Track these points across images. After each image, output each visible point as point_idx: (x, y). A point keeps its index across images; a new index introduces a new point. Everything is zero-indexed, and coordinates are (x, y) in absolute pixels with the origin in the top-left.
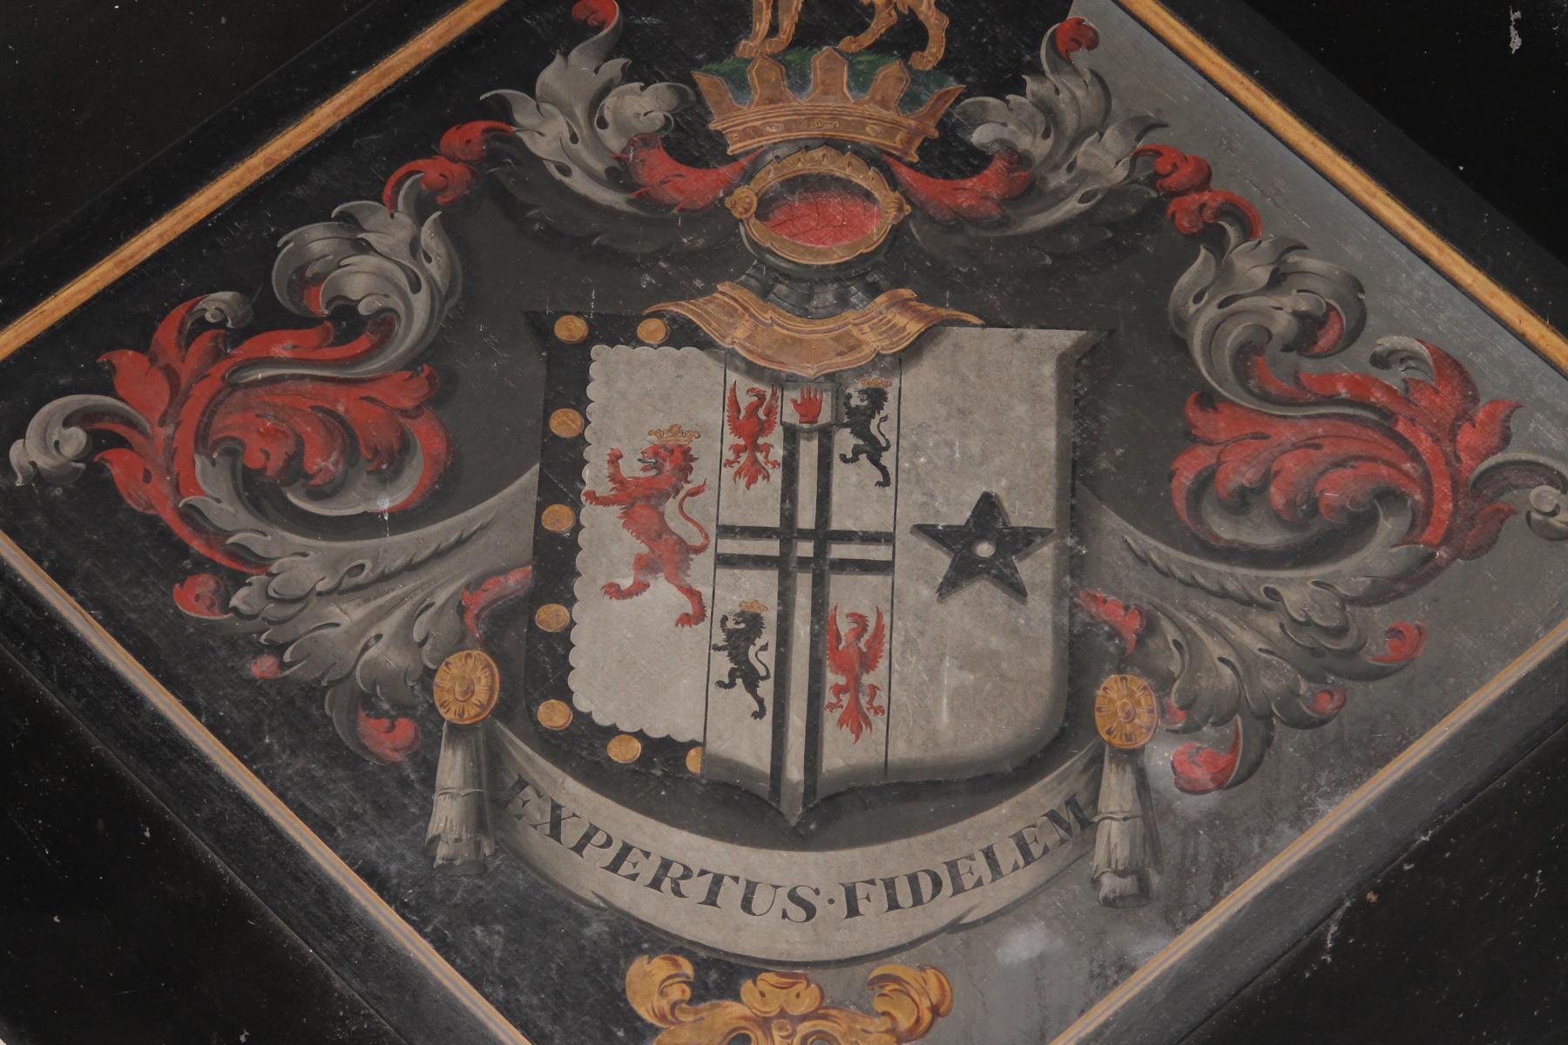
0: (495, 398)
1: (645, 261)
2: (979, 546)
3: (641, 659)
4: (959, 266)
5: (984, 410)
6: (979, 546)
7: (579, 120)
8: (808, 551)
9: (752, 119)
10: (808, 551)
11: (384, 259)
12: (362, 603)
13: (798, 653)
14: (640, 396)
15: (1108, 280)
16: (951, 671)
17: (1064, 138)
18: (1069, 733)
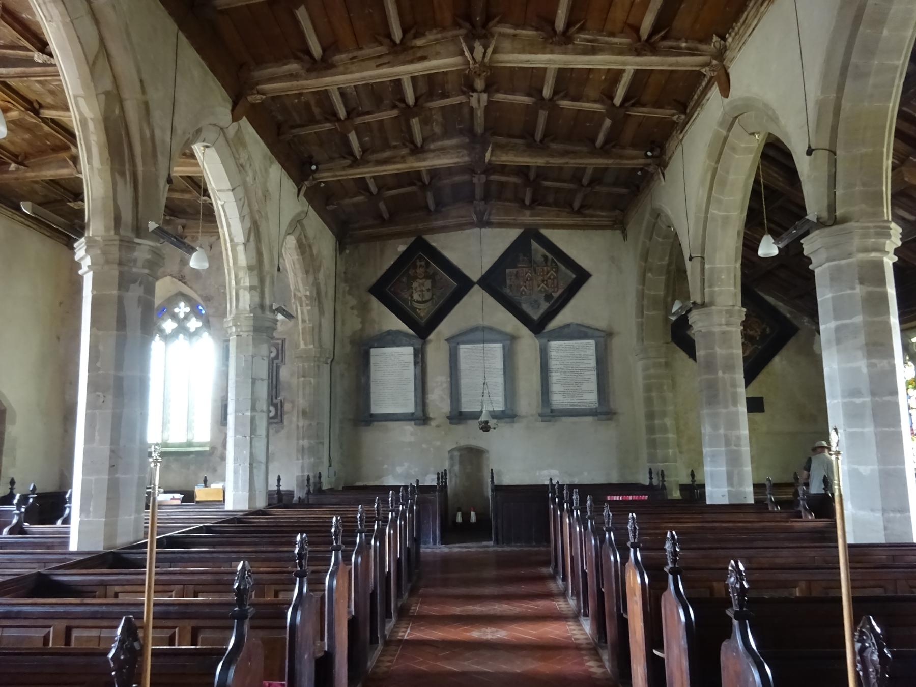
0: (409, 286)
1: (415, 278)
2: (428, 290)
3: (416, 296)
4: (427, 277)
5: (428, 284)
6: (428, 290)
7: (411, 272)
8: (422, 291)
9: (418, 271)
10: (422, 291)
11: (404, 280)
12: (406, 296)
13: (422, 295)
14: (415, 285)
15: (431, 277)
16: (428, 296)
17: (431, 271)
18: (432, 299)
